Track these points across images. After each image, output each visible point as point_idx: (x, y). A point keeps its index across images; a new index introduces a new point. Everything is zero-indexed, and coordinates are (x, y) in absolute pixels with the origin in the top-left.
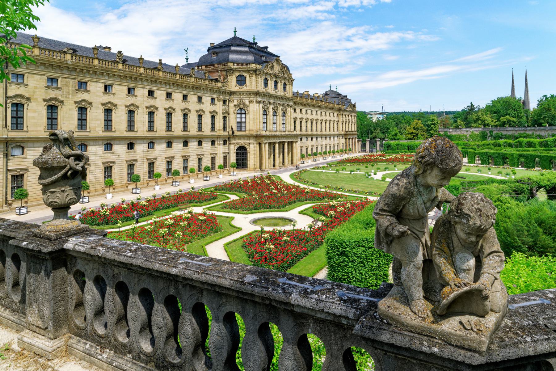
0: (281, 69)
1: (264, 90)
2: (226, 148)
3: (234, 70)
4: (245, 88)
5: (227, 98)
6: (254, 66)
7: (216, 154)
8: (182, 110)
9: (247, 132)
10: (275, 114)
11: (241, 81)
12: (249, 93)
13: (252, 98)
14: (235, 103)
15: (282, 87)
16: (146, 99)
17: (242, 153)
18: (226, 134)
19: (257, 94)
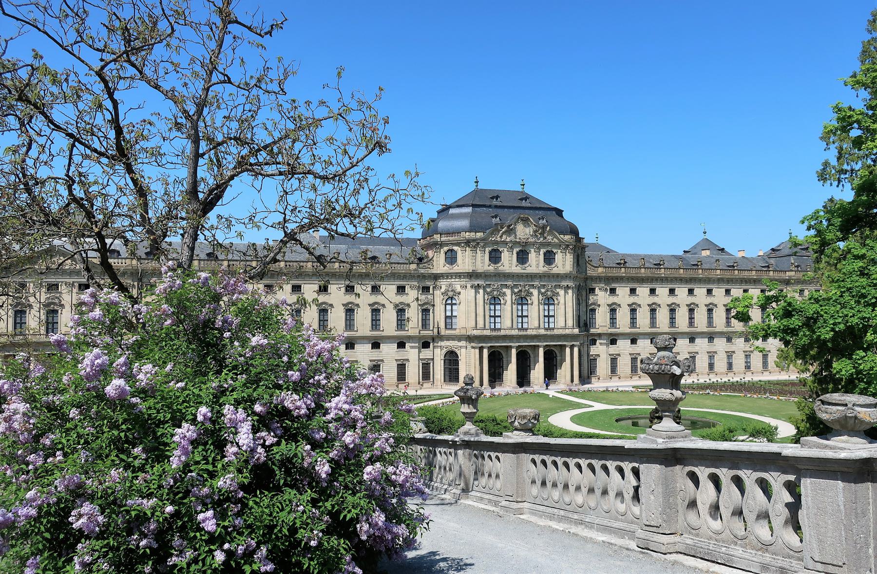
0: (535, 232)
1: (491, 268)
3: (442, 245)
4: (456, 269)
5: (428, 283)
6: (467, 235)
7: (407, 360)
8: (343, 305)
9: (458, 331)
10: (522, 300)
11: (451, 258)
12: (459, 275)
13: (463, 281)
14: (443, 290)
17: (452, 360)
18: (430, 333)
19: (472, 275)
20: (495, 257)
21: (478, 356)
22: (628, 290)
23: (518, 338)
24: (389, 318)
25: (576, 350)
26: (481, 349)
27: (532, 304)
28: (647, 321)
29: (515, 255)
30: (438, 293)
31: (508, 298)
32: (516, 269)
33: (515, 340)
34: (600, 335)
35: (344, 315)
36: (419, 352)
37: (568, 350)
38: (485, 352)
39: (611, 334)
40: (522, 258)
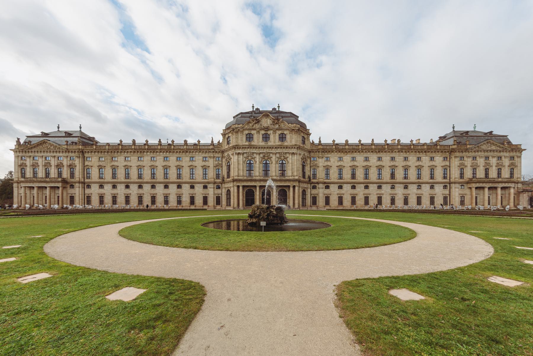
1: (247, 143)
2: (219, 191)
15: (277, 137)
16: (149, 162)
19: (236, 147)
20: (250, 137)
21: (236, 190)
22: (337, 158)
23: (260, 180)
24: (199, 172)
25: (297, 188)
26: (238, 187)
27: (272, 163)
28: (349, 176)
29: (261, 136)
30: (224, 160)
31: (257, 159)
32: (262, 144)
33: (258, 183)
34: (318, 183)
35: (176, 171)
36: (214, 191)
37: (291, 189)
38: (241, 188)
39: (325, 183)
40: (266, 138)
